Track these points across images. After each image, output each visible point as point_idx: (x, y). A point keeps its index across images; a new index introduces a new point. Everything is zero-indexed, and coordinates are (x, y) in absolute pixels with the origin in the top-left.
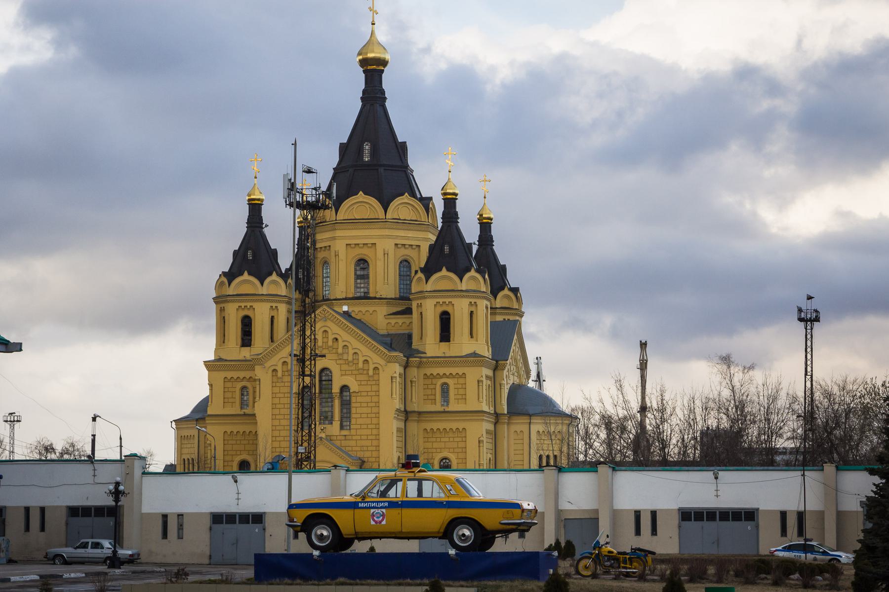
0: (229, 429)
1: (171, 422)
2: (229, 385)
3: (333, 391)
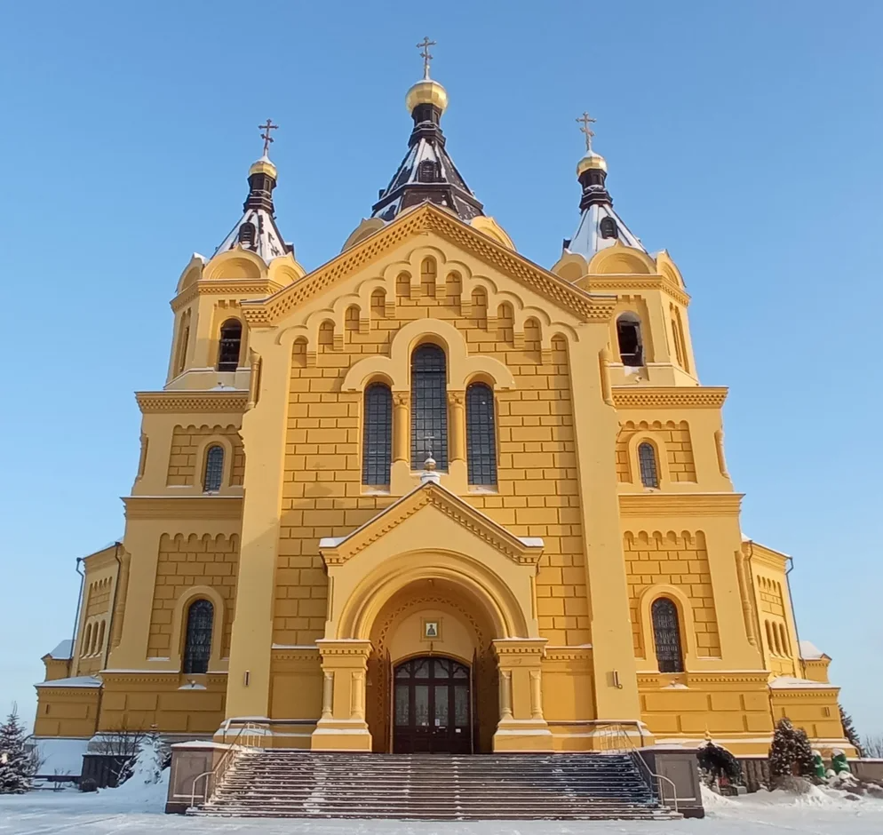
0: (172, 527)
1: (79, 560)
2: (182, 440)
3: (449, 387)
